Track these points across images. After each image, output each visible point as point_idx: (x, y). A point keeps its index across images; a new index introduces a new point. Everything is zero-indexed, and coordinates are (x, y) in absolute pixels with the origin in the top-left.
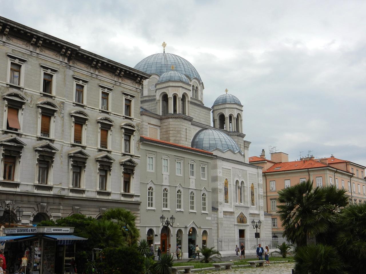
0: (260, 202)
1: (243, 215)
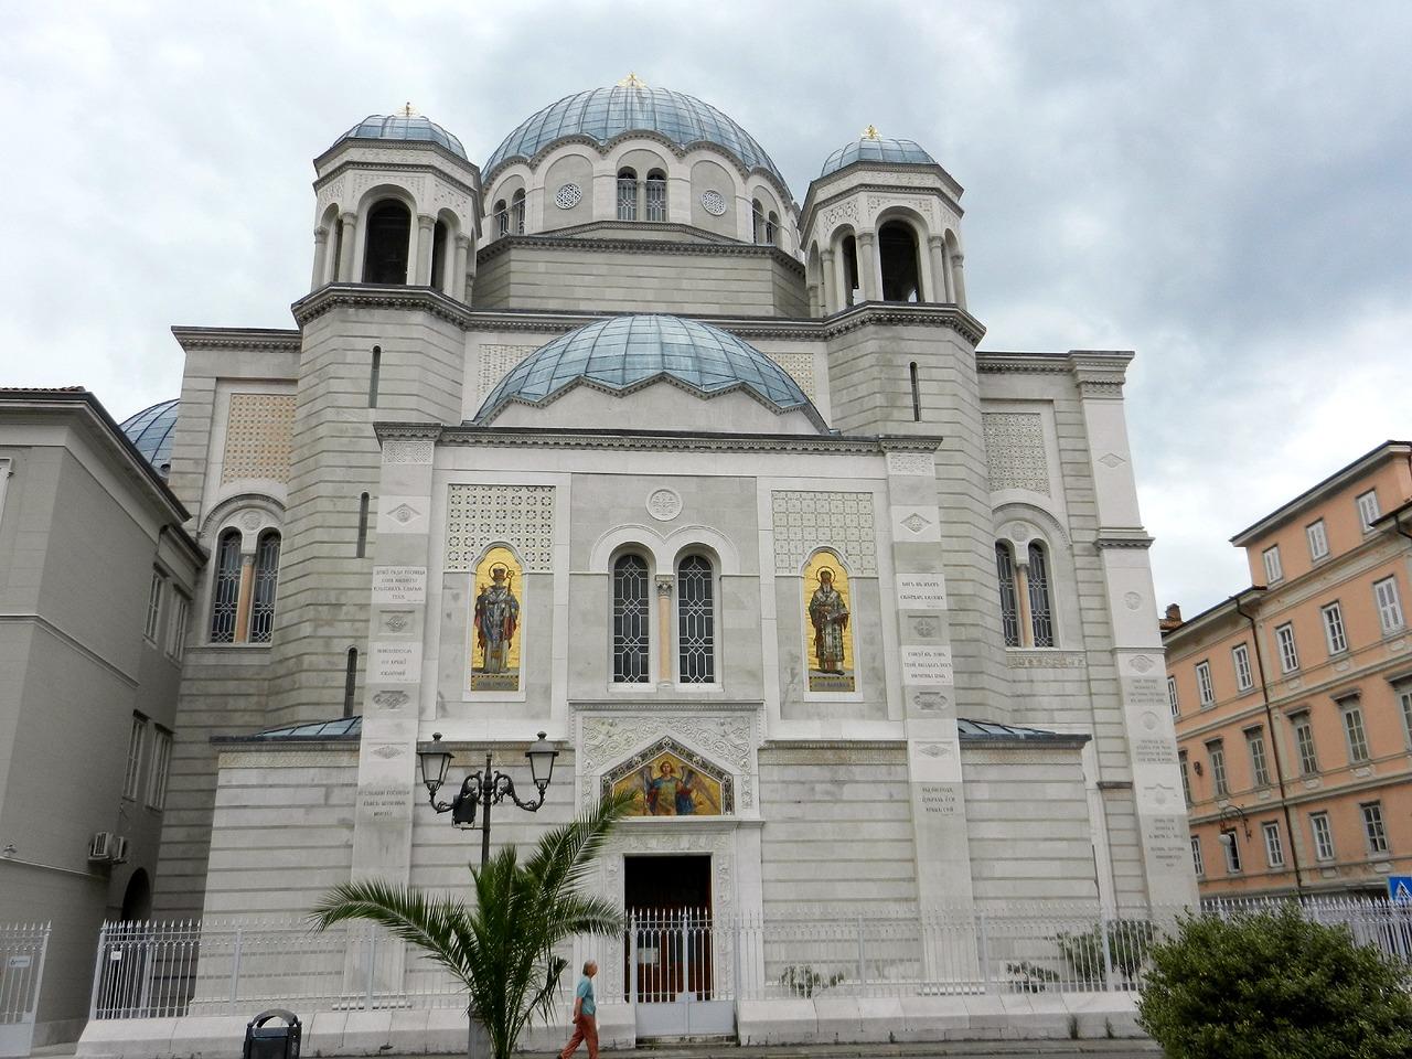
0: (907, 659)
1: (690, 756)
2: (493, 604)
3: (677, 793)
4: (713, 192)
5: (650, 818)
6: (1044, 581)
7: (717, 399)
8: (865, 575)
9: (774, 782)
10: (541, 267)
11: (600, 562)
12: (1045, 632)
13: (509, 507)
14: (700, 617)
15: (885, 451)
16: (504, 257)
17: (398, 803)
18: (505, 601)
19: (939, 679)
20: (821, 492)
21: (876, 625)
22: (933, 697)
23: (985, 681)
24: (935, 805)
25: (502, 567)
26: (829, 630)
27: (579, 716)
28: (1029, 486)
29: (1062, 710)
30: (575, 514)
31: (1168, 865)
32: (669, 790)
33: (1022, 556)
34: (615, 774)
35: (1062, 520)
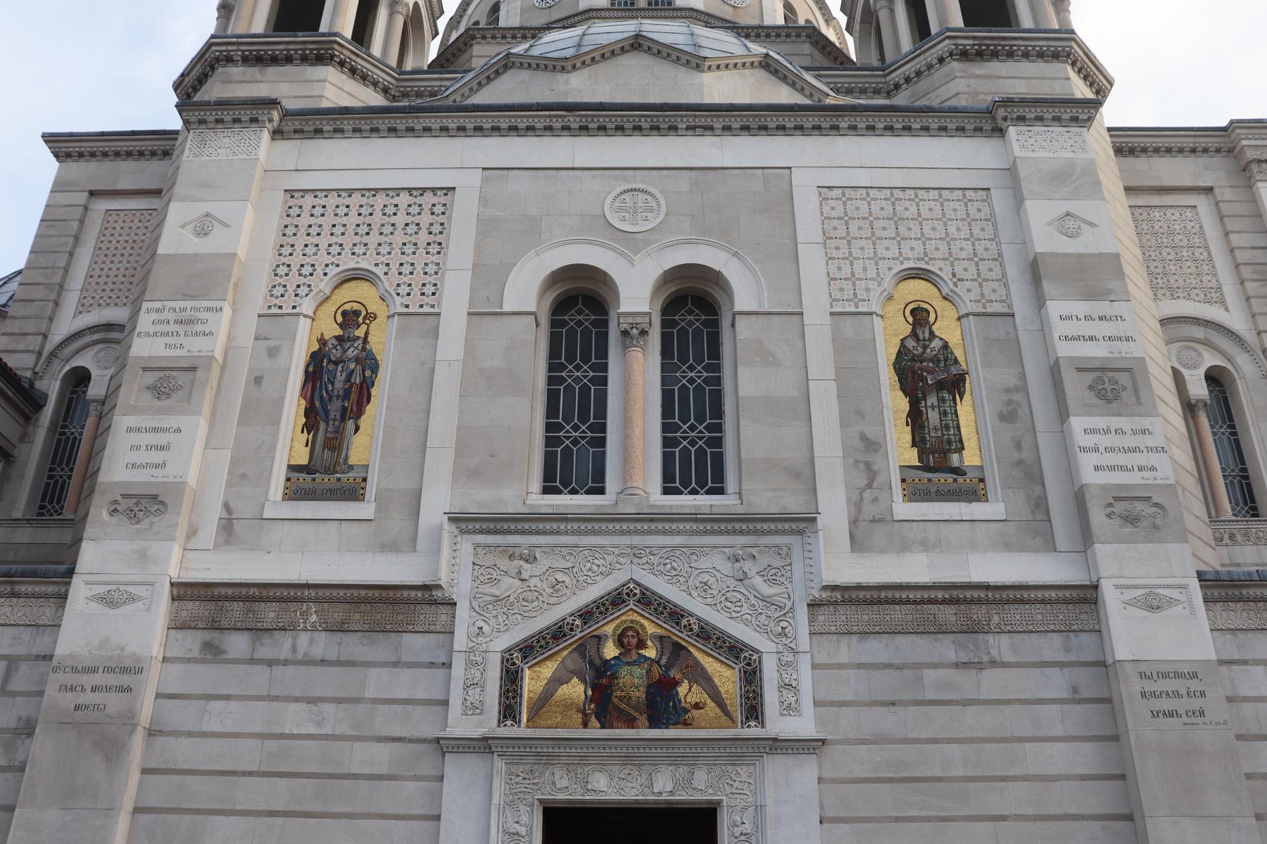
0: (1082, 440)
1: (676, 615)
2: (336, 363)
3: (649, 687)
5: (596, 732)
6: (1233, 427)
8: (989, 310)
9: (841, 666)
13: (377, 219)
14: (699, 389)
15: (1004, 125)
16: (466, 56)
17: (121, 689)
18: (357, 360)
19: (1145, 474)
20: (903, 189)
21: (1017, 389)
22: (1139, 506)
25: (356, 307)
26: (932, 400)
28: (1193, 296)
30: (486, 227)
32: (633, 681)
34: (531, 647)
35: (1249, 336)
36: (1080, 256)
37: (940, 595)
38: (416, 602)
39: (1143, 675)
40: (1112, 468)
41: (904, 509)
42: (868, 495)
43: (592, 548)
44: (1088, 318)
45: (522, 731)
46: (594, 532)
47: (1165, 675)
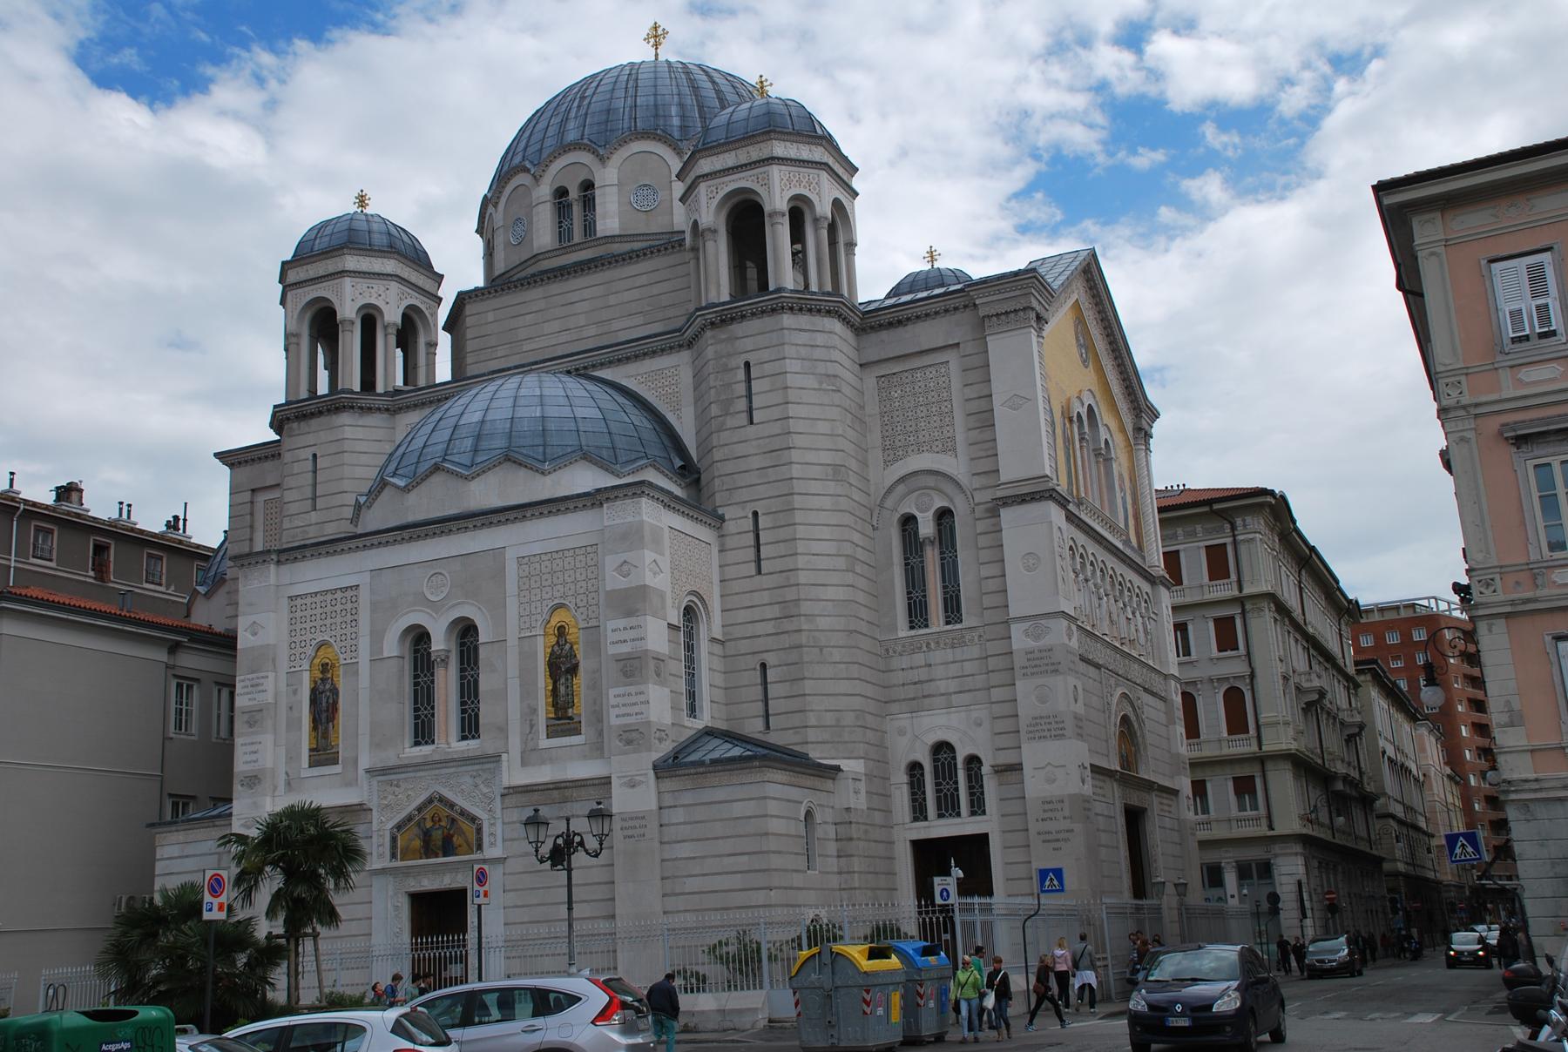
0: (613, 701)
1: (452, 805)
4: (645, 185)
7: (483, 477)
8: (590, 625)
10: (490, 317)
11: (392, 645)
12: (953, 609)
18: (330, 690)
19: (639, 717)
20: (557, 552)
22: (634, 735)
23: (809, 686)
24: (630, 832)
25: (327, 661)
26: (563, 680)
27: (374, 782)
29: (960, 692)
30: (375, 607)
31: (1054, 849)
32: (437, 835)
33: (926, 528)
35: (964, 479)
36: (626, 589)
37: (551, 786)
38: (359, 810)
39: (623, 820)
40: (624, 715)
41: (544, 743)
42: (530, 736)
43: (420, 777)
44: (625, 629)
45: (399, 864)
46: (419, 771)
47: (632, 819)
